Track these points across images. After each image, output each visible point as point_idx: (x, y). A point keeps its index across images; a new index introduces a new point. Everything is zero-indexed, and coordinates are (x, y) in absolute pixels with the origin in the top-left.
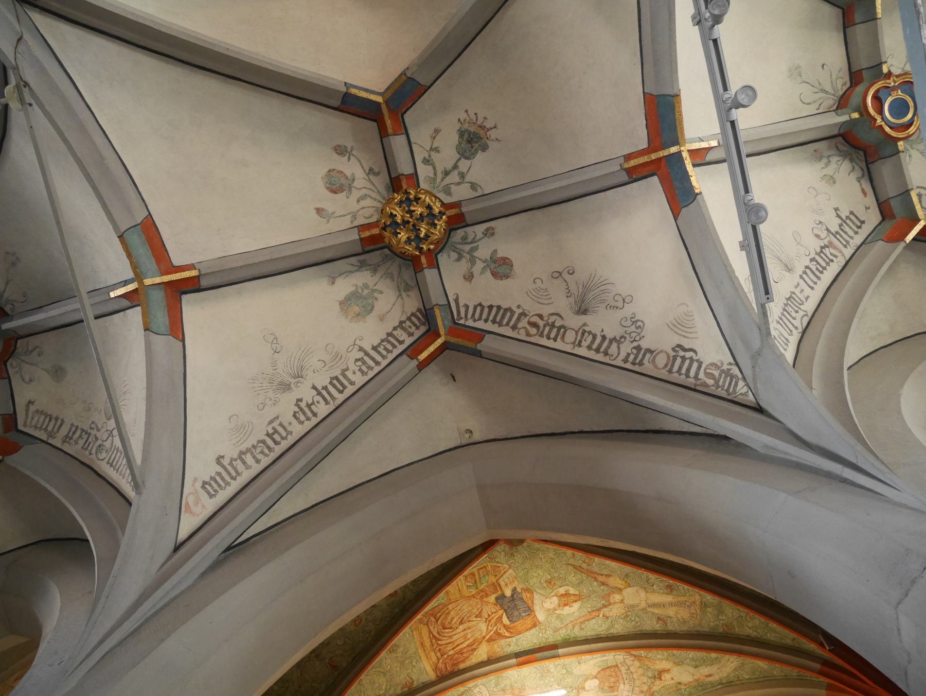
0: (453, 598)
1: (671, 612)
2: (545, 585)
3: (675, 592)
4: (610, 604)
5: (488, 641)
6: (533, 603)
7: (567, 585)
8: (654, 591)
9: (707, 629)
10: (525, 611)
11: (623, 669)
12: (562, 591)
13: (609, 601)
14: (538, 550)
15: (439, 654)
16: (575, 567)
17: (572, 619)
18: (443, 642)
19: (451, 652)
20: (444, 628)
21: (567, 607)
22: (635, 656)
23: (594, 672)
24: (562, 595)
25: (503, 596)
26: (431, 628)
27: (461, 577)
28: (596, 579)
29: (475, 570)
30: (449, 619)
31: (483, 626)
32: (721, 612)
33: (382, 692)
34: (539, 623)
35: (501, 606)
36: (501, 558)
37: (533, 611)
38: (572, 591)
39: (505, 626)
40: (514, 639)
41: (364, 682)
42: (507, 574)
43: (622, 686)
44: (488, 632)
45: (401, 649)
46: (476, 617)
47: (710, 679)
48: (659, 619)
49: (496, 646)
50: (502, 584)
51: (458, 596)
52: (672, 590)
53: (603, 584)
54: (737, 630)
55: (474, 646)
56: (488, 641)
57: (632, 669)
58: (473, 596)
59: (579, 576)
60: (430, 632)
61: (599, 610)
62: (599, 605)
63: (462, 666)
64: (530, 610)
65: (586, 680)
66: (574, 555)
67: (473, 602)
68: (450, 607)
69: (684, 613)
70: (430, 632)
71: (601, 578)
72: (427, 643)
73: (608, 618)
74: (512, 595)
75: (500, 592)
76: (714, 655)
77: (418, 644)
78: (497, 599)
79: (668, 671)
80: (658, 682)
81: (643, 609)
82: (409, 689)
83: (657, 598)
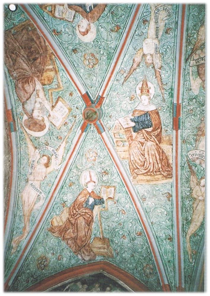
1: (161, 25)
3: (148, 19)
4: (153, 63)
5: (160, 143)
8: (147, 33)
10: (147, 117)
12: (139, 92)
13: (150, 64)
15: (158, 173)
16: (125, 81)
17: (159, 89)
18: (152, 168)
19: (160, 165)
20: (144, 166)
21: (150, 91)
24: (142, 92)
26: (141, 173)
28: (135, 69)
30: (138, 161)
31: (149, 144)
34: (157, 109)
36: (111, 123)
38: (140, 85)
39: (153, 131)
40: (163, 127)
45: (146, 194)
46: (142, 146)
48: (166, 32)
50: (126, 126)
51: (127, 153)
53: (138, 65)
55: (161, 152)
56: (160, 143)
60: (143, 174)
62: (153, 71)
64: (146, 114)
68: (132, 159)
70: (143, 174)
72: (149, 178)
73: (162, 67)
74: (135, 122)
75: (131, 129)
78: (135, 131)
81: (159, 41)
83: (152, 31)
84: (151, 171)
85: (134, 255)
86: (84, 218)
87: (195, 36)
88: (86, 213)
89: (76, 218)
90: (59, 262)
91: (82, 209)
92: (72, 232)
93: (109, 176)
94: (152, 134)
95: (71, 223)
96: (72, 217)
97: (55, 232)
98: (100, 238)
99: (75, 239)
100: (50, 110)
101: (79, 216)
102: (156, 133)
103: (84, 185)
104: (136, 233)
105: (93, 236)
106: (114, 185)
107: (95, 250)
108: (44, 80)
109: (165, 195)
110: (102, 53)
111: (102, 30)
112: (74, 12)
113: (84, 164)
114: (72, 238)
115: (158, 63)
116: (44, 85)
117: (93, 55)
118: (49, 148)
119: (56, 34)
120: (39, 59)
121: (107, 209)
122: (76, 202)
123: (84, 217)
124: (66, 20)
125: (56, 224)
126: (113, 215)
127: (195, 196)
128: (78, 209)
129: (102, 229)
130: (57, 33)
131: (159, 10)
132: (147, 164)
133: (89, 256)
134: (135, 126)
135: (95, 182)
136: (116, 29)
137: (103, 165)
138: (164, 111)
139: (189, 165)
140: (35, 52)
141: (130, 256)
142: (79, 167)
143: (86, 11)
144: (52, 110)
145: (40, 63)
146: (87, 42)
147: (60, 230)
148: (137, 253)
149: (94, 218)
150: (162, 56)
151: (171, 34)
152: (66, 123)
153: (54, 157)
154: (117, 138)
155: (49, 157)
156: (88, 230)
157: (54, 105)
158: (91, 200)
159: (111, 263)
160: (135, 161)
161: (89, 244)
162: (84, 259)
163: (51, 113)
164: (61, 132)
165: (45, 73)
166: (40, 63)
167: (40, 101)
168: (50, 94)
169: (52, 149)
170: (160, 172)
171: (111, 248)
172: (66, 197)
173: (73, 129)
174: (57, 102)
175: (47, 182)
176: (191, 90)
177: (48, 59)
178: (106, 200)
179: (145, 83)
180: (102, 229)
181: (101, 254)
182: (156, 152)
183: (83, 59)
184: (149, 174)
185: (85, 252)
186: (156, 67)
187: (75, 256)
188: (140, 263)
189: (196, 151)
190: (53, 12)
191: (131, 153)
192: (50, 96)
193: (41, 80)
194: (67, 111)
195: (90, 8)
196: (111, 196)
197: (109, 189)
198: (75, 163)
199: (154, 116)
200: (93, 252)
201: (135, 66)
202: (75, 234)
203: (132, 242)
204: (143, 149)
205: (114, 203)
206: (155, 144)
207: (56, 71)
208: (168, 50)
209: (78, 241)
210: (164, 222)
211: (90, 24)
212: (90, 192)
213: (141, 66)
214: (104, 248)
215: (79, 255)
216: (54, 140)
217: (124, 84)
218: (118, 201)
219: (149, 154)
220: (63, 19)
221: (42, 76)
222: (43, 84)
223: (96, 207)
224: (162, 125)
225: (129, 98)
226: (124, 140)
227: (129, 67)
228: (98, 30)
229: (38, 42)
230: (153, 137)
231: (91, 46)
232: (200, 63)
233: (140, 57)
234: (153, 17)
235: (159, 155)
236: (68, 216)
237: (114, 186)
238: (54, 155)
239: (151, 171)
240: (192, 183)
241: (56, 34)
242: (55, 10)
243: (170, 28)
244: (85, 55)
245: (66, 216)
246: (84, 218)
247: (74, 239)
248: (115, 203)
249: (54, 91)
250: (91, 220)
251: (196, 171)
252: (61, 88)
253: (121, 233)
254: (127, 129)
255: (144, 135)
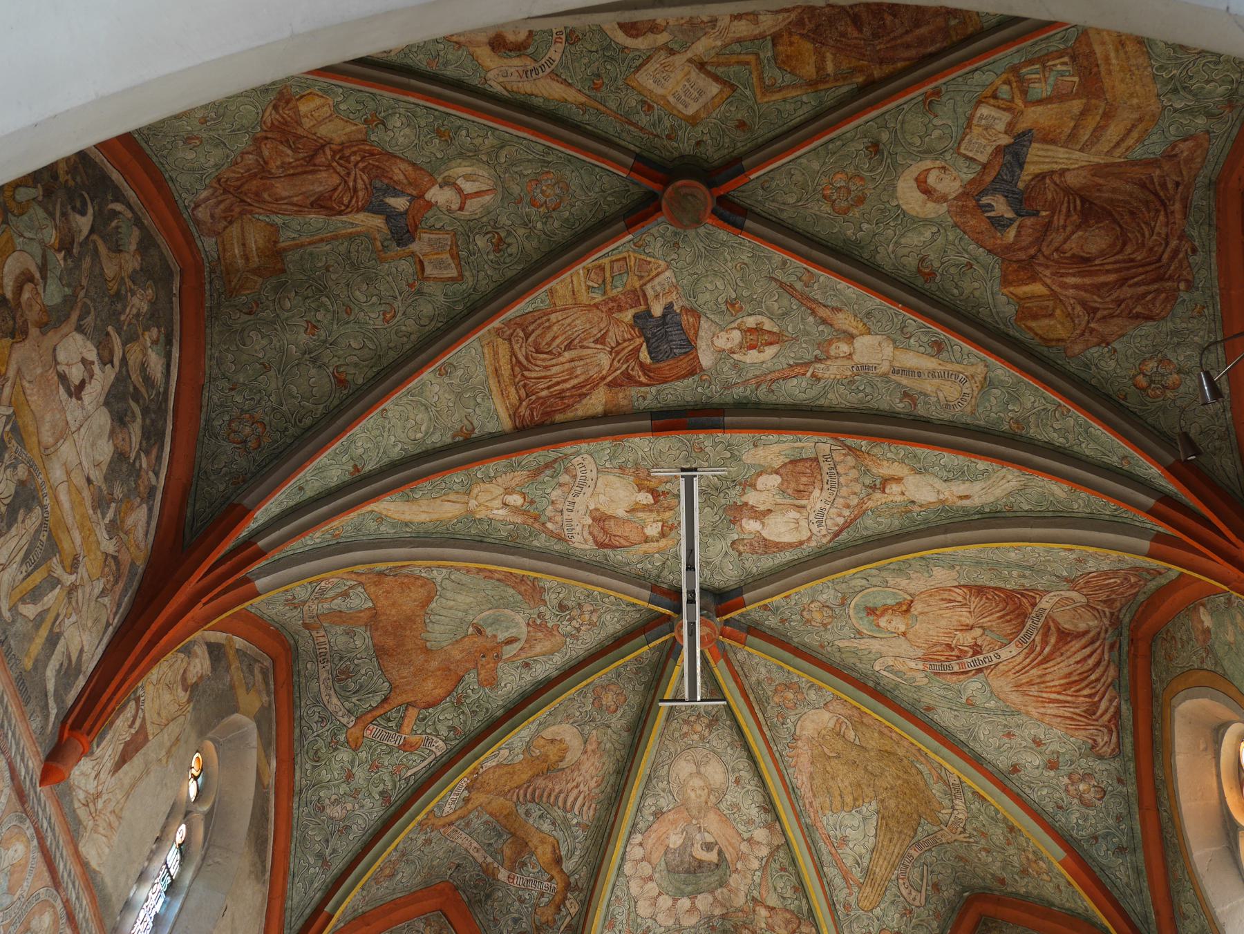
0: (560, 303)
1: (928, 386)
2: (724, 308)
3: (945, 354)
4: (828, 358)
5: (609, 385)
6: (696, 334)
7: (761, 314)
8: (908, 348)
9: (982, 423)
10: (681, 347)
11: (825, 467)
12: (751, 322)
13: (828, 352)
14: (723, 244)
15: (523, 393)
16: (782, 285)
18: (534, 375)
19: (544, 393)
20: (537, 352)
21: (754, 353)
22: (850, 448)
23: (777, 464)
24: (750, 330)
25: (648, 314)
26: (516, 347)
27: (579, 268)
28: (813, 313)
29: (606, 261)
30: (549, 336)
31: (605, 360)
32: (1014, 397)
33: (419, 435)
34: (702, 370)
35: (642, 330)
36: (656, 247)
37: (695, 348)
38: (768, 325)
39: (642, 365)
40: (654, 389)
41: (390, 414)
42: (662, 277)
43: (816, 493)
44: (612, 369)
45: (460, 372)
46: (596, 342)
47: (966, 503)
48: (906, 394)
49: (621, 395)
50: (650, 292)
51: (570, 301)
52: (940, 350)
53: (824, 322)
54: (1033, 432)
55: (584, 390)
56: (609, 385)
57: (840, 469)
58: (596, 306)
59: (785, 302)
60: (513, 353)
61: (807, 364)
62: (809, 357)
63: (559, 418)
64: (690, 346)
65: (760, 474)
66: (784, 263)
67: (595, 315)
68: (553, 317)
69: (950, 391)
70: (513, 353)
71: (823, 312)
72: (506, 371)
73: (819, 379)
74: (664, 316)
76: (982, 465)
77: (490, 370)
78: (636, 317)
79: (899, 480)
80: (878, 495)
81: (884, 375)
82: (466, 439)
83: (911, 360)
84: (526, 373)
85: (272, 373)
86: (335, 189)
87: (889, 455)
88: (355, 190)
89: (335, 164)
90: (181, 143)
91: (365, 178)
92: (283, 163)
93: (491, 257)
94: (632, 363)
95: (314, 153)
96: (334, 153)
97: (277, 112)
98: (276, 242)
99: (263, 171)
100: (689, 54)
101: (343, 173)
102: (637, 373)
103: (446, 174)
104: (337, 367)
105: (278, 220)
106: (467, 274)
107: (235, 230)
108: (791, 44)
109: (466, 422)
110: (865, 226)
111: (928, 234)
112: (983, 158)
113: (516, 169)
114: (266, 163)
115: (830, 371)
116: (773, 40)
117: (861, 200)
118: (560, 47)
119: (927, 98)
120: (856, 34)
121: (383, 261)
122: (385, 158)
123: (340, 188)
124: (965, 134)
125: (304, 108)
126: (369, 280)
127: (475, 491)
128: (365, 168)
129: (310, 244)
130: (930, 103)
131: (963, 382)
132: (543, 360)
133: (212, 216)
134: (652, 316)
135: (461, 208)
136: (927, 271)
137: (521, 231)
138: (699, 389)
139: (555, 461)
140: (879, 27)
141: (260, 356)
142: (504, 153)
143: (983, 193)
144: (690, 61)
145: (843, 35)
146: (899, 189)
147: (286, 123)
148: (280, 384)
149: (344, 218)
150: (845, 382)
151: (901, 405)
152: (650, 107)
153: (530, 65)
154: (612, 268)
155: (526, 48)
156: (296, 205)
157: (709, 68)
158: (399, 203)
159: (207, 287)
160: (549, 327)
161: (251, 212)
162: (197, 206)
163: (679, 59)
164: (617, 88)
165: (810, 46)
166: (843, 35)
167: (718, 24)
168: (742, 57)
169: (557, 57)
170: (527, 396)
171: (256, 282)
172: (398, 124)
173: (631, 128)
174: (716, 78)
175: (442, 53)
176: (755, 446)
177: (854, 63)
178: (413, 254)
179: (776, 339)
180: (310, 244)
181: (224, 250)
182: (581, 379)
183: (851, 171)
184: (517, 369)
185: (222, 206)
186: (817, 366)
187: (207, 181)
188: (257, 397)
189: (595, 471)
190: (992, 101)
191: (570, 312)
192: (734, 58)
193: (790, 34)
194: (690, 111)
195: (990, 205)
196: (429, 271)
197: (450, 261)
198: (516, 139)
199: (684, 364)
200: (226, 227)
201: (823, 312)
202: (279, 172)
203: (307, 356)
204: (585, 343)
205: (411, 281)
206: (604, 372)
207: (817, 83)
208: (861, 395)
209: (255, 184)
210: (393, 439)
211: (946, 201)
212: (428, 196)
213: (821, 328)
214: (246, 258)
215: (211, 191)
216: (587, 66)
217: (774, 283)
218: (420, 293)
219: (572, 360)
220: (969, 126)
221: (802, 35)
222: (776, 39)
223: (378, 222)
224: (659, 387)
225: (734, 295)
226: (608, 287)
227: (819, 297)
228: (927, 222)
229: (908, 38)
230: (625, 366)
231: (885, 198)
232: (822, 464)
233: (845, 327)
234: (949, 367)
235: (573, 387)
236: (338, 140)
237: (461, 275)
238: (537, 65)
239: (526, 373)
240: (509, 476)
241: (927, 98)
242: (999, 107)
243: (915, 405)
244: (862, 179)
245: (334, 135)
246: (335, 189)
247: (263, 170)
248: (410, 286)
249: (755, 75)
250: (332, 209)
251: (540, 478)
252: (764, 94)
253: (319, 316)
254: (640, 293)
255: (625, 344)
